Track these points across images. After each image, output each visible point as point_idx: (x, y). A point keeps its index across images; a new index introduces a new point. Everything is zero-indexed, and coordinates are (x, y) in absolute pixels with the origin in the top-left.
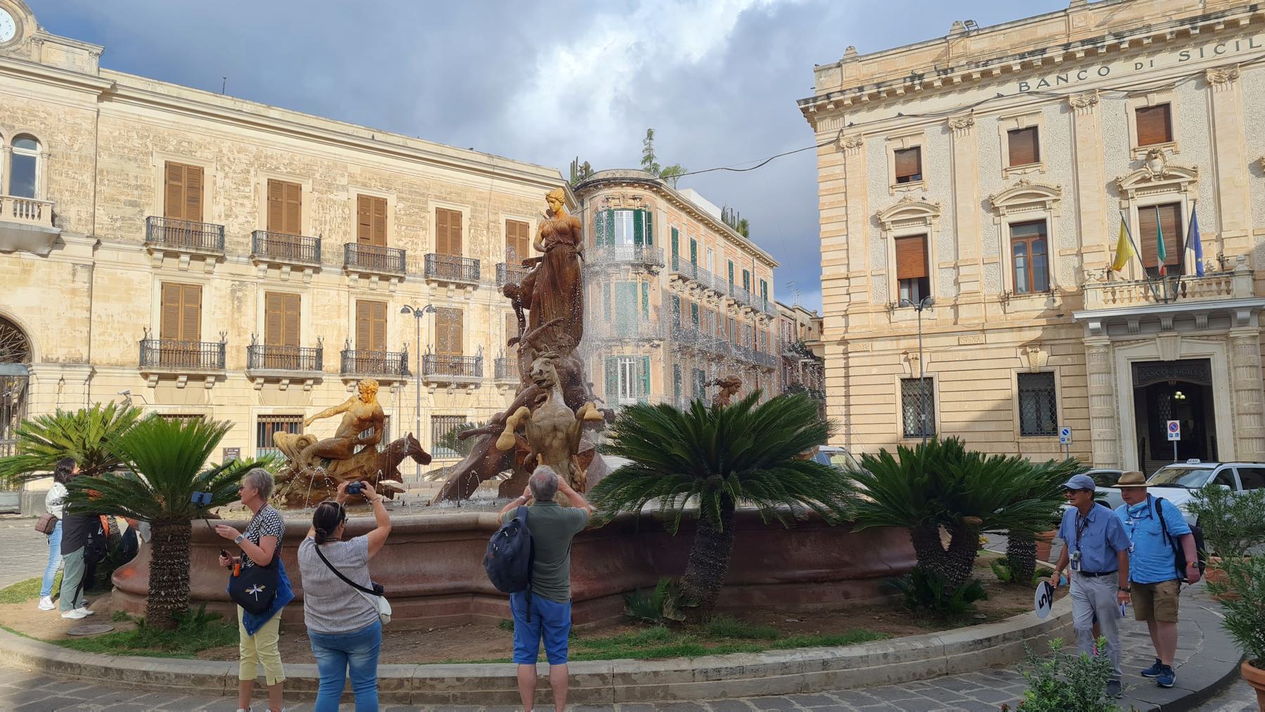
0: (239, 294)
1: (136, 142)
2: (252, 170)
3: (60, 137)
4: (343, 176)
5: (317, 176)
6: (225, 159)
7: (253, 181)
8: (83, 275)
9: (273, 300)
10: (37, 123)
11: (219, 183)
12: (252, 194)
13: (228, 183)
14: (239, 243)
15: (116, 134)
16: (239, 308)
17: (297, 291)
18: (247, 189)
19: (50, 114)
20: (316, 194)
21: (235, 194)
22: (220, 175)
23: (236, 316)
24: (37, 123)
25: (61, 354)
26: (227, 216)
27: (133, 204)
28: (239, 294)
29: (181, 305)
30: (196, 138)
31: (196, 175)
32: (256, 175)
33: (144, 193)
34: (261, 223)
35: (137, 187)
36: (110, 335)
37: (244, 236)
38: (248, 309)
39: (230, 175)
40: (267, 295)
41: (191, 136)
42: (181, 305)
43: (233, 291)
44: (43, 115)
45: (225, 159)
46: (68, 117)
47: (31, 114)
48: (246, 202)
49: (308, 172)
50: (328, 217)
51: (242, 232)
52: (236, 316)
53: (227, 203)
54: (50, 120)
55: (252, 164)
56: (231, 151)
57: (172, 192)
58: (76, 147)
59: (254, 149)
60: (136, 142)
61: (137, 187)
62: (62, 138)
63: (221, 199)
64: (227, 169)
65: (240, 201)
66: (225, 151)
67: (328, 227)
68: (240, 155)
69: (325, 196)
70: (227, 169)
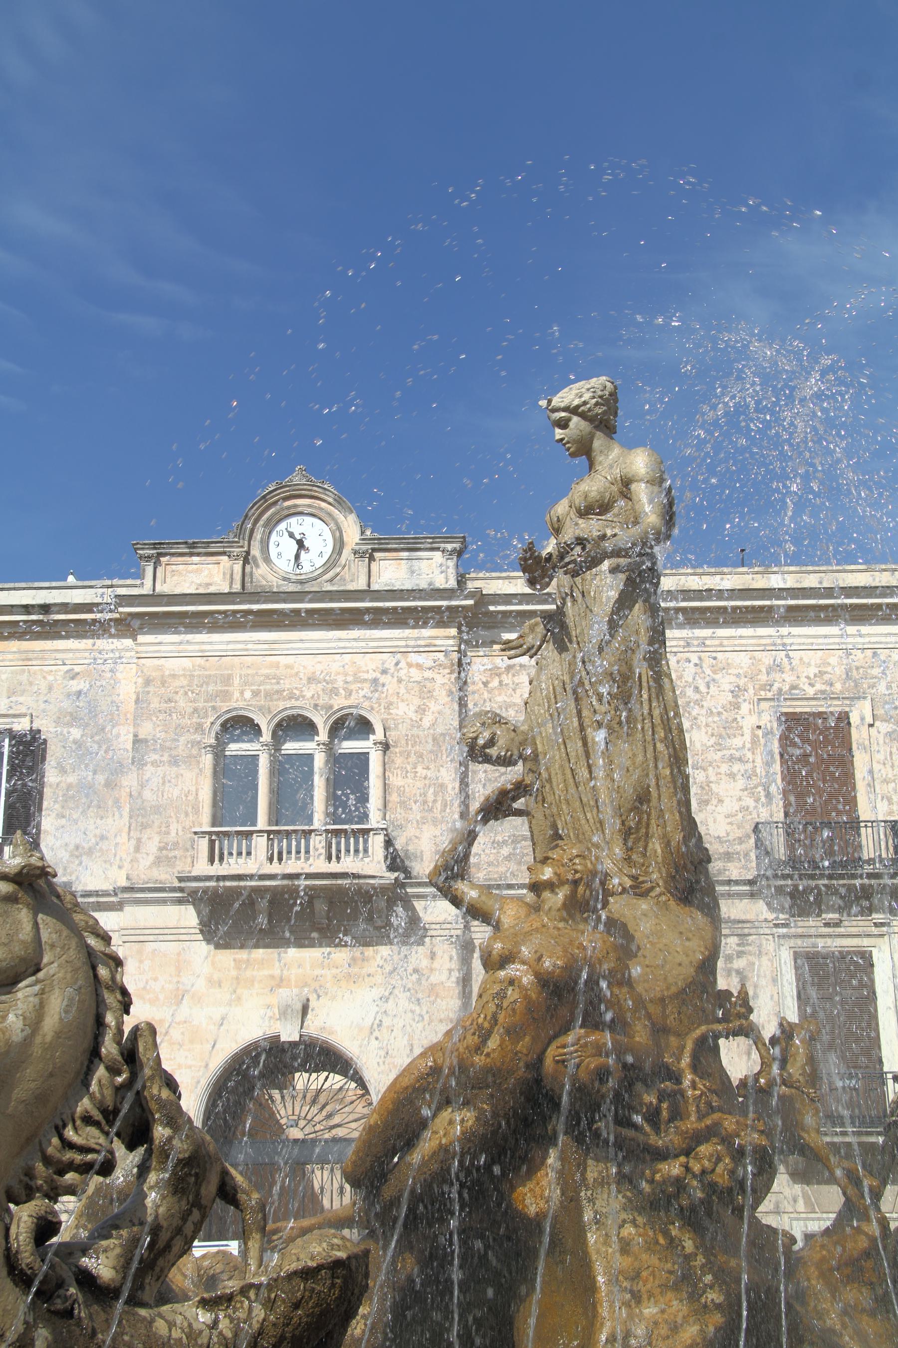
3: (402, 706)
7: (749, 722)
18: (737, 742)
39: (702, 720)
47: (358, 680)
58: (426, 722)
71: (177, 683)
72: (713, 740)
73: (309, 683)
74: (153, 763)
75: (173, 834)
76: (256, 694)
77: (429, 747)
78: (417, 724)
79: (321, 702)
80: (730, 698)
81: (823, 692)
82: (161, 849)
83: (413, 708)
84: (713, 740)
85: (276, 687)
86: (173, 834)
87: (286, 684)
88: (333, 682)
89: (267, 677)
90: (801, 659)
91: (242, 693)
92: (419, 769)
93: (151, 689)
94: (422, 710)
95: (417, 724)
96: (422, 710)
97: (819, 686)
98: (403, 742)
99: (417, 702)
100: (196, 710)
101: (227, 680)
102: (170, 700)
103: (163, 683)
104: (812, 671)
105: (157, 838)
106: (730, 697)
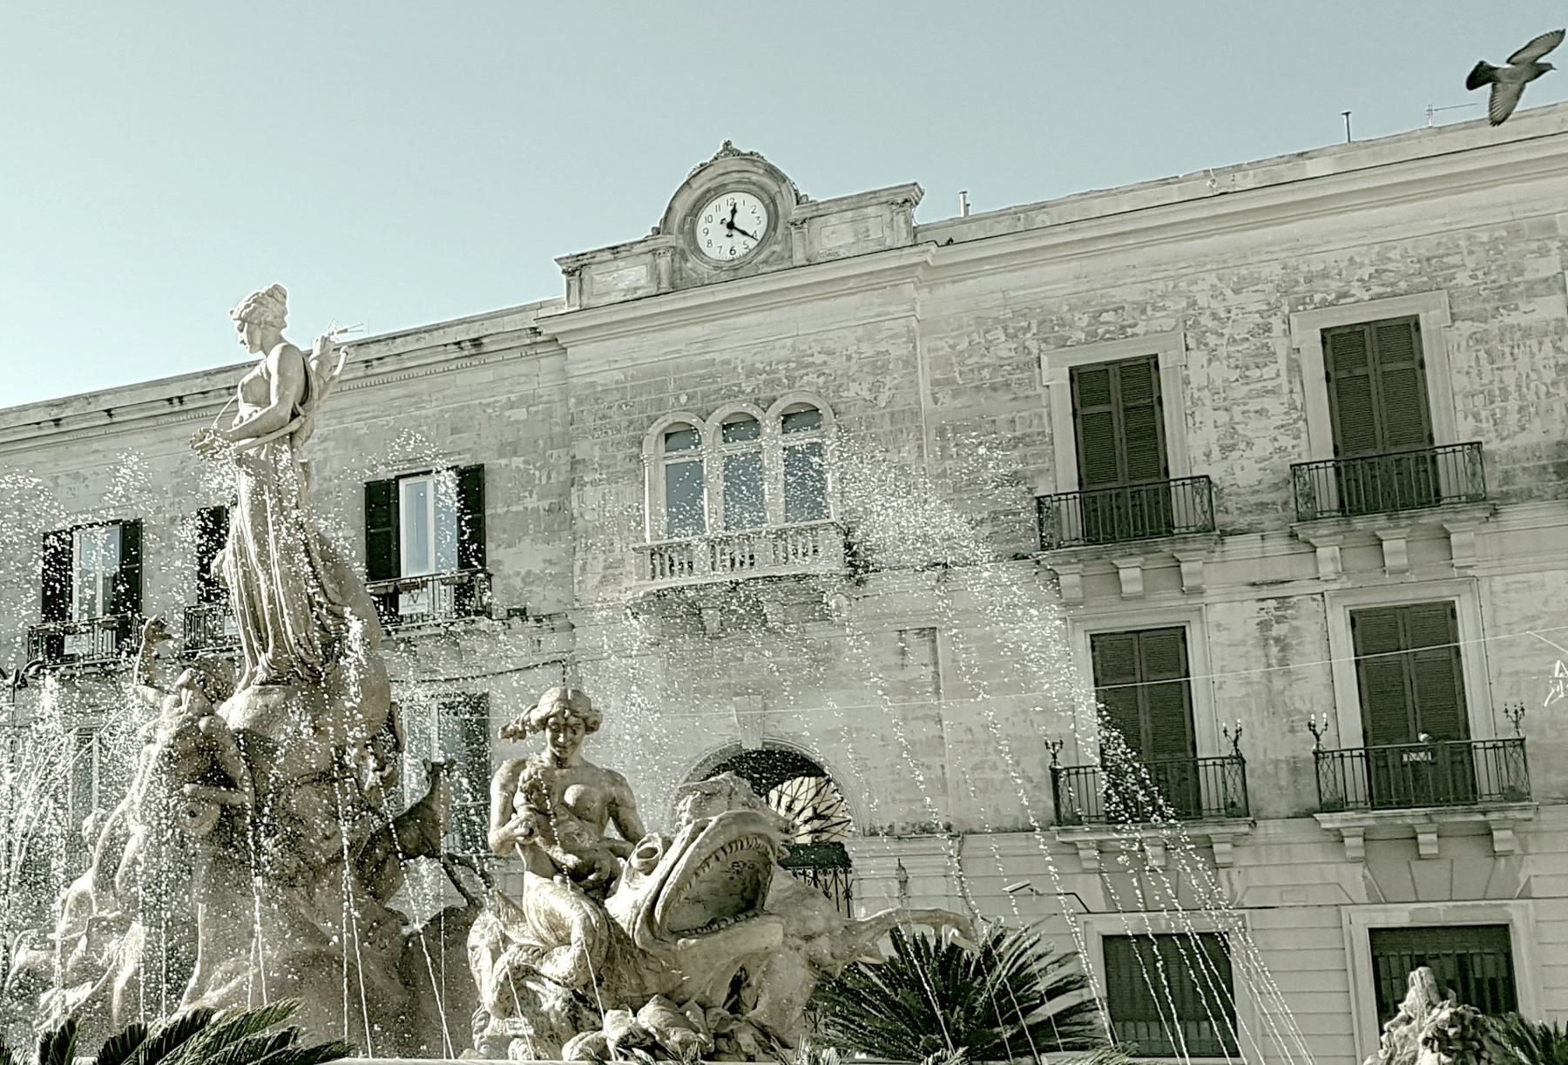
0: (1278, 630)
1: (1005, 349)
2: (1277, 324)
3: (854, 387)
4: (1543, 252)
5: (1462, 278)
6: (1206, 320)
7: (1281, 348)
8: (919, 651)
9: (1370, 629)
10: (812, 377)
11: (1197, 378)
12: (1284, 379)
13: (1221, 372)
14: (1262, 507)
15: (964, 345)
16: (1283, 662)
17: (1443, 593)
18: (1268, 372)
19: (831, 353)
20: (1466, 327)
21: (1240, 391)
22: (1198, 357)
23: (1278, 684)
24: (812, 377)
25: (897, 815)
26: (1226, 449)
27: (1015, 479)
28: (1278, 630)
29: (1143, 678)
30: (1129, 294)
31: (1143, 372)
32: (1288, 332)
33: (1032, 450)
34: (1317, 440)
35: (1016, 442)
36: (994, 767)
37: (1276, 487)
38: (1308, 664)
39: (1222, 352)
40: (1355, 619)
41: (1118, 295)
42: (1143, 678)
43: (1264, 625)
44: (819, 359)
45: (1206, 320)
46: (864, 347)
48: (1269, 403)
49: (1433, 273)
50: (1510, 379)
51: (1270, 478)
52: (1278, 684)
53: (1223, 417)
54: (836, 364)
55: (1274, 309)
56: (1217, 294)
57: (1089, 430)
59: (1277, 268)
60: (1005, 349)
61: (1016, 442)
62: (856, 391)
63: (1206, 414)
64: (1212, 340)
65: (1254, 405)
66: (1202, 301)
67: (1513, 404)
68: (1241, 298)
69: (1493, 326)
70: (1212, 340)
71: (609, 398)
72: (1236, 374)
73: (748, 376)
74: (593, 483)
75: (617, 551)
76: (690, 398)
77: (888, 428)
78: (873, 403)
79: (762, 395)
80: (1260, 320)
81: (1380, 296)
82: (606, 568)
83: (866, 386)
84: (1236, 374)
85: (713, 387)
86: (617, 551)
87: (722, 382)
88: (774, 372)
89: (703, 377)
90: (1351, 259)
91: (677, 398)
92: (879, 456)
93: (585, 407)
94: (875, 388)
95: (873, 403)
96: (875, 388)
97: (1376, 290)
98: (856, 426)
99: (871, 379)
100: (631, 422)
101: (661, 388)
102: (604, 417)
103: (596, 400)
104: (1365, 273)
105: (601, 557)
106: (1257, 318)
